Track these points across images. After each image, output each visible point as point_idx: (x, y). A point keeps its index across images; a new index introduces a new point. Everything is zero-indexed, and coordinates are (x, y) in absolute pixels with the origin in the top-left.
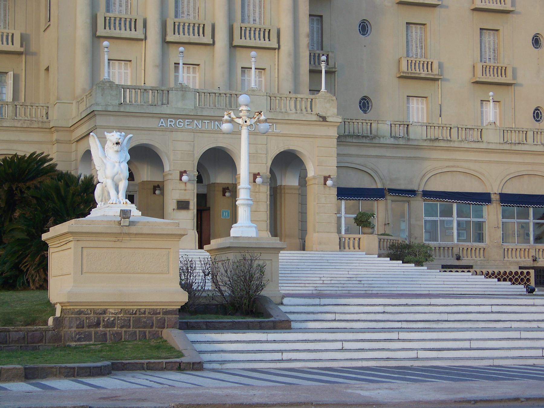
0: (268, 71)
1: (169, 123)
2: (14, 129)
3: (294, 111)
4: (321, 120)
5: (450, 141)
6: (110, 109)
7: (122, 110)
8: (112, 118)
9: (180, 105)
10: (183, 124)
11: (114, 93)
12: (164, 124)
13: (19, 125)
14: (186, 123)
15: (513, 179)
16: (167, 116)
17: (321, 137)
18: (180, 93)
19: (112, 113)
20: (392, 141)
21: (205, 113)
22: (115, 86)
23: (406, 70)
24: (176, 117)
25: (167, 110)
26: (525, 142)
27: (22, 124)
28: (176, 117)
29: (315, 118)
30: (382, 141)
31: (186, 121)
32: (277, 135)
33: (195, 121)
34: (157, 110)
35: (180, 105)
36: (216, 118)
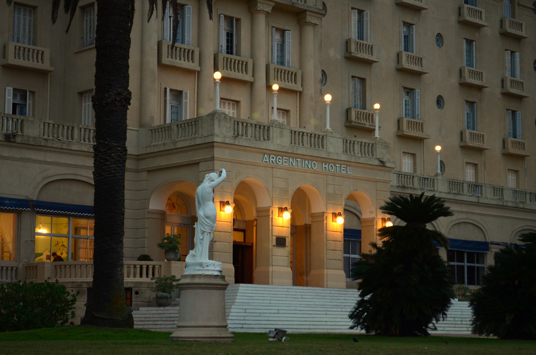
1: (271, 159)
2: (81, 153)
3: (360, 155)
4: (382, 165)
5: (415, 189)
7: (236, 143)
9: (278, 141)
10: (282, 162)
11: (228, 125)
12: (267, 160)
13: (86, 150)
14: (284, 160)
15: (471, 227)
16: (270, 152)
17: (379, 181)
18: (279, 130)
19: (228, 146)
21: (299, 152)
22: (228, 118)
23: (354, 120)
24: (277, 153)
26: (461, 193)
27: (88, 148)
28: (277, 153)
29: (377, 163)
31: (284, 158)
33: (291, 160)
35: (278, 141)
36: (306, 157)
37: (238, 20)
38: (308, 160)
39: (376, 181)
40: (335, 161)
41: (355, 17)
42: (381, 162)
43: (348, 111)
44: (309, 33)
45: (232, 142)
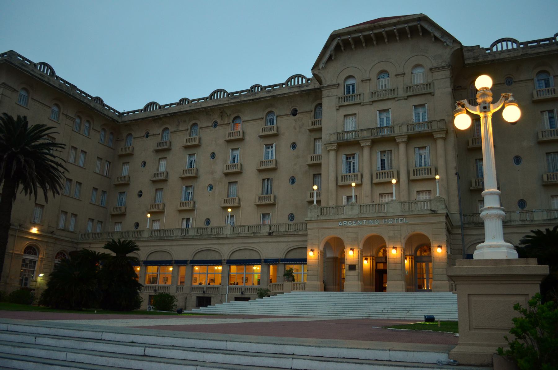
0: (432, 192)
6: (313, 219)
7: (319, 219)
8: (315, 224)
9: (350, 213)
10: (352, 223)
11: (316, 211)
17: (435, 223)
20: (520, 223)
21: (363, 216)
24: (347, 220)
25: (343, 217)
28: (347, 220)
29: (429, 212)
30: (513, 223)
32: (407, 225)
34: (337, 217)
37: (391, 151)
38: (371, 220)
39: (432, 223)
40: (393, 217)
41: (546, 116)
42: (433, 211)
43: (542, 177)
44: (440, 143)
45: (316, 219)
